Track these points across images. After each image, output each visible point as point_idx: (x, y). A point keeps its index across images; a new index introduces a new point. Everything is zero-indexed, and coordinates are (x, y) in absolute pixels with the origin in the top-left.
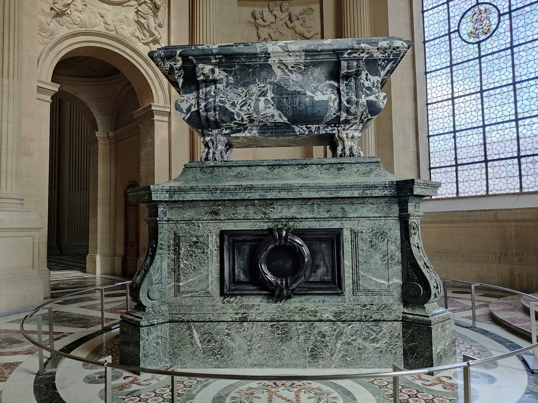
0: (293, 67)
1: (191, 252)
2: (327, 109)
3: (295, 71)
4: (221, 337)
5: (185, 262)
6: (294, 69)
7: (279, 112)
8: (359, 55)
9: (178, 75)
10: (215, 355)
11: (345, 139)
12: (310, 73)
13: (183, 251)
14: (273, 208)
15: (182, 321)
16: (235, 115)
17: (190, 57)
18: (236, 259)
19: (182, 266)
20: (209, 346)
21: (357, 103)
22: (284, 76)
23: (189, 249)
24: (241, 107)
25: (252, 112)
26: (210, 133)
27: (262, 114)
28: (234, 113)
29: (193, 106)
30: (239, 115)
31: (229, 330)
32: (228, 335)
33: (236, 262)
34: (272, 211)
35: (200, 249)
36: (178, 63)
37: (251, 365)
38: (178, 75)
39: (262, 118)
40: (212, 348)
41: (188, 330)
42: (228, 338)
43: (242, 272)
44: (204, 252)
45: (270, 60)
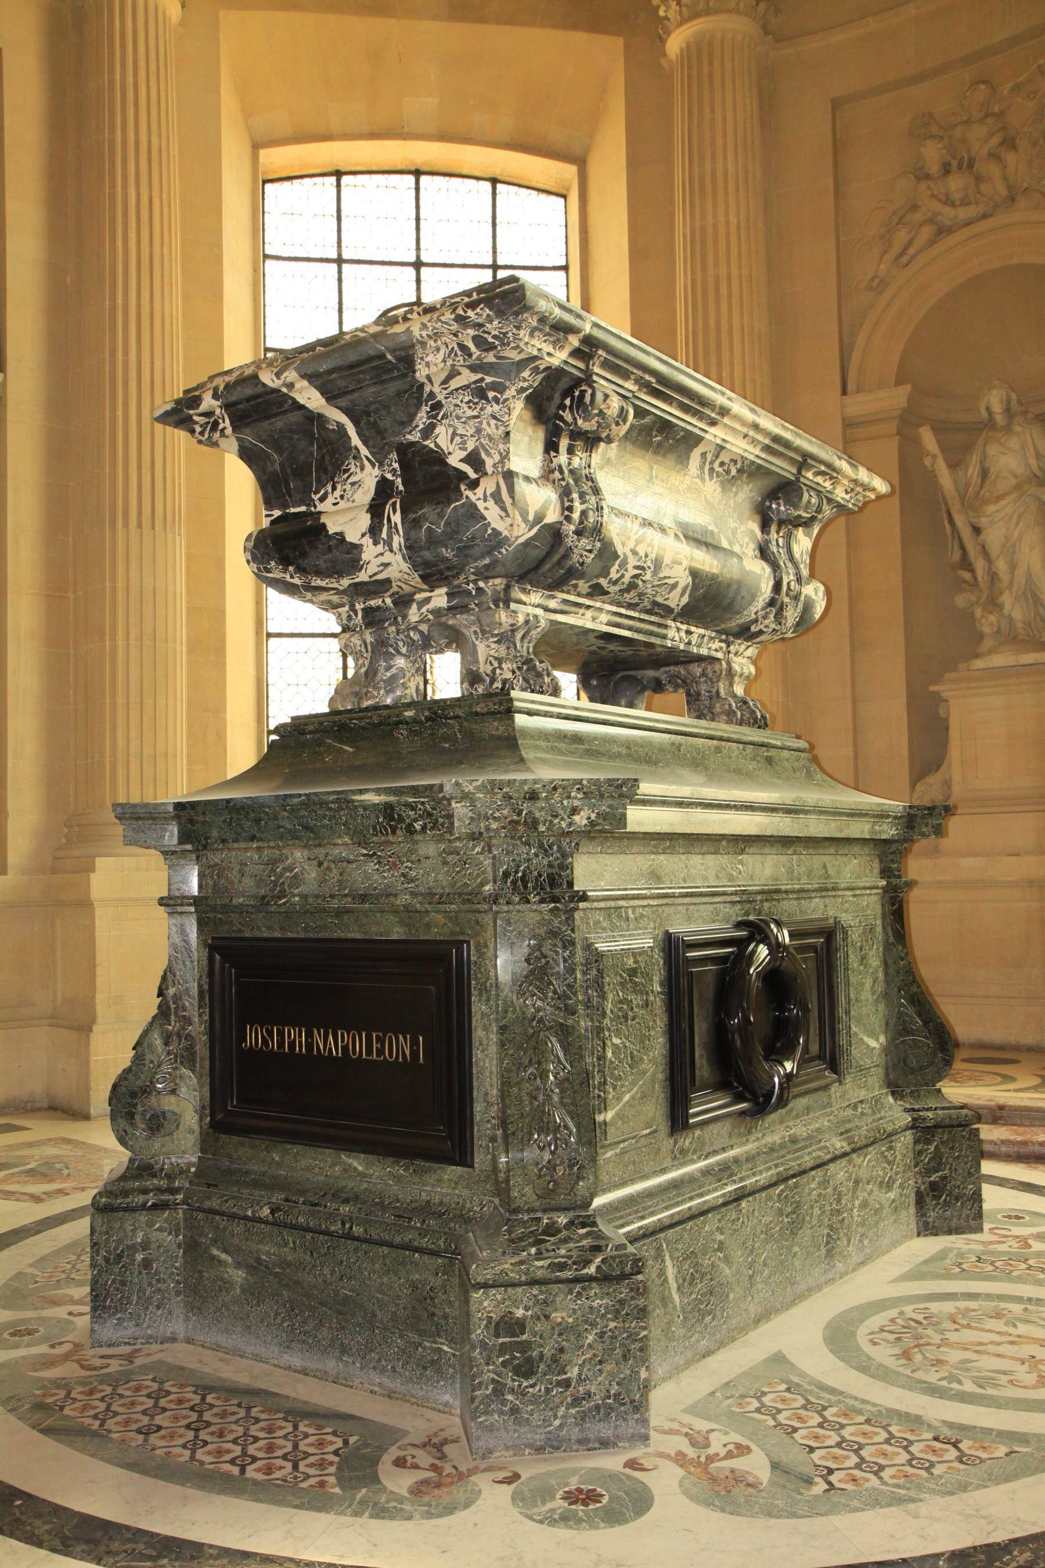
0: (722, 464)
1: (625, 1007)
2: (753, 597)
3: (718, 476)
4: (709, 1259)
5: (616, 1041)
6: (720, 470)
7: (690, 579)
8: (825, 481)
9: (521, 384)
10: (703, 1319)
11: (736, 679)
12: (734, 489)
13: (610, 1005)
14: (741, 862)
15: (645, 1236)
16: (618, 562)
17: (600, 352)
18: (696, 1019)
19: (609, 1054)
20: (693, 1296)
21: (796, 598)
22: (698, 480)
23: (621, 994)
24: (638, 542)
25: (649, 563)
26: (524, 598)
27: (662, 575)
28: (619, 557)
29: (552, 508)
30: (624, 564)
31: (722, 1233)
32: (720, 1249)
33: (696, 1028)
34: (740, 873)
35: (641, 992)
36: (558, 354)
37: (754, 1322)
38: (521, 384)
39: (653, 586)
40: (696, 1299)
41: (656, 1258)
42: (721, 1255)
43: (705, 1057)
44: (647, 1004)
45: (712, 430)
